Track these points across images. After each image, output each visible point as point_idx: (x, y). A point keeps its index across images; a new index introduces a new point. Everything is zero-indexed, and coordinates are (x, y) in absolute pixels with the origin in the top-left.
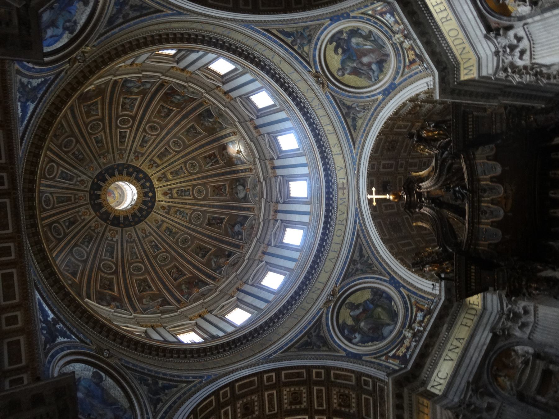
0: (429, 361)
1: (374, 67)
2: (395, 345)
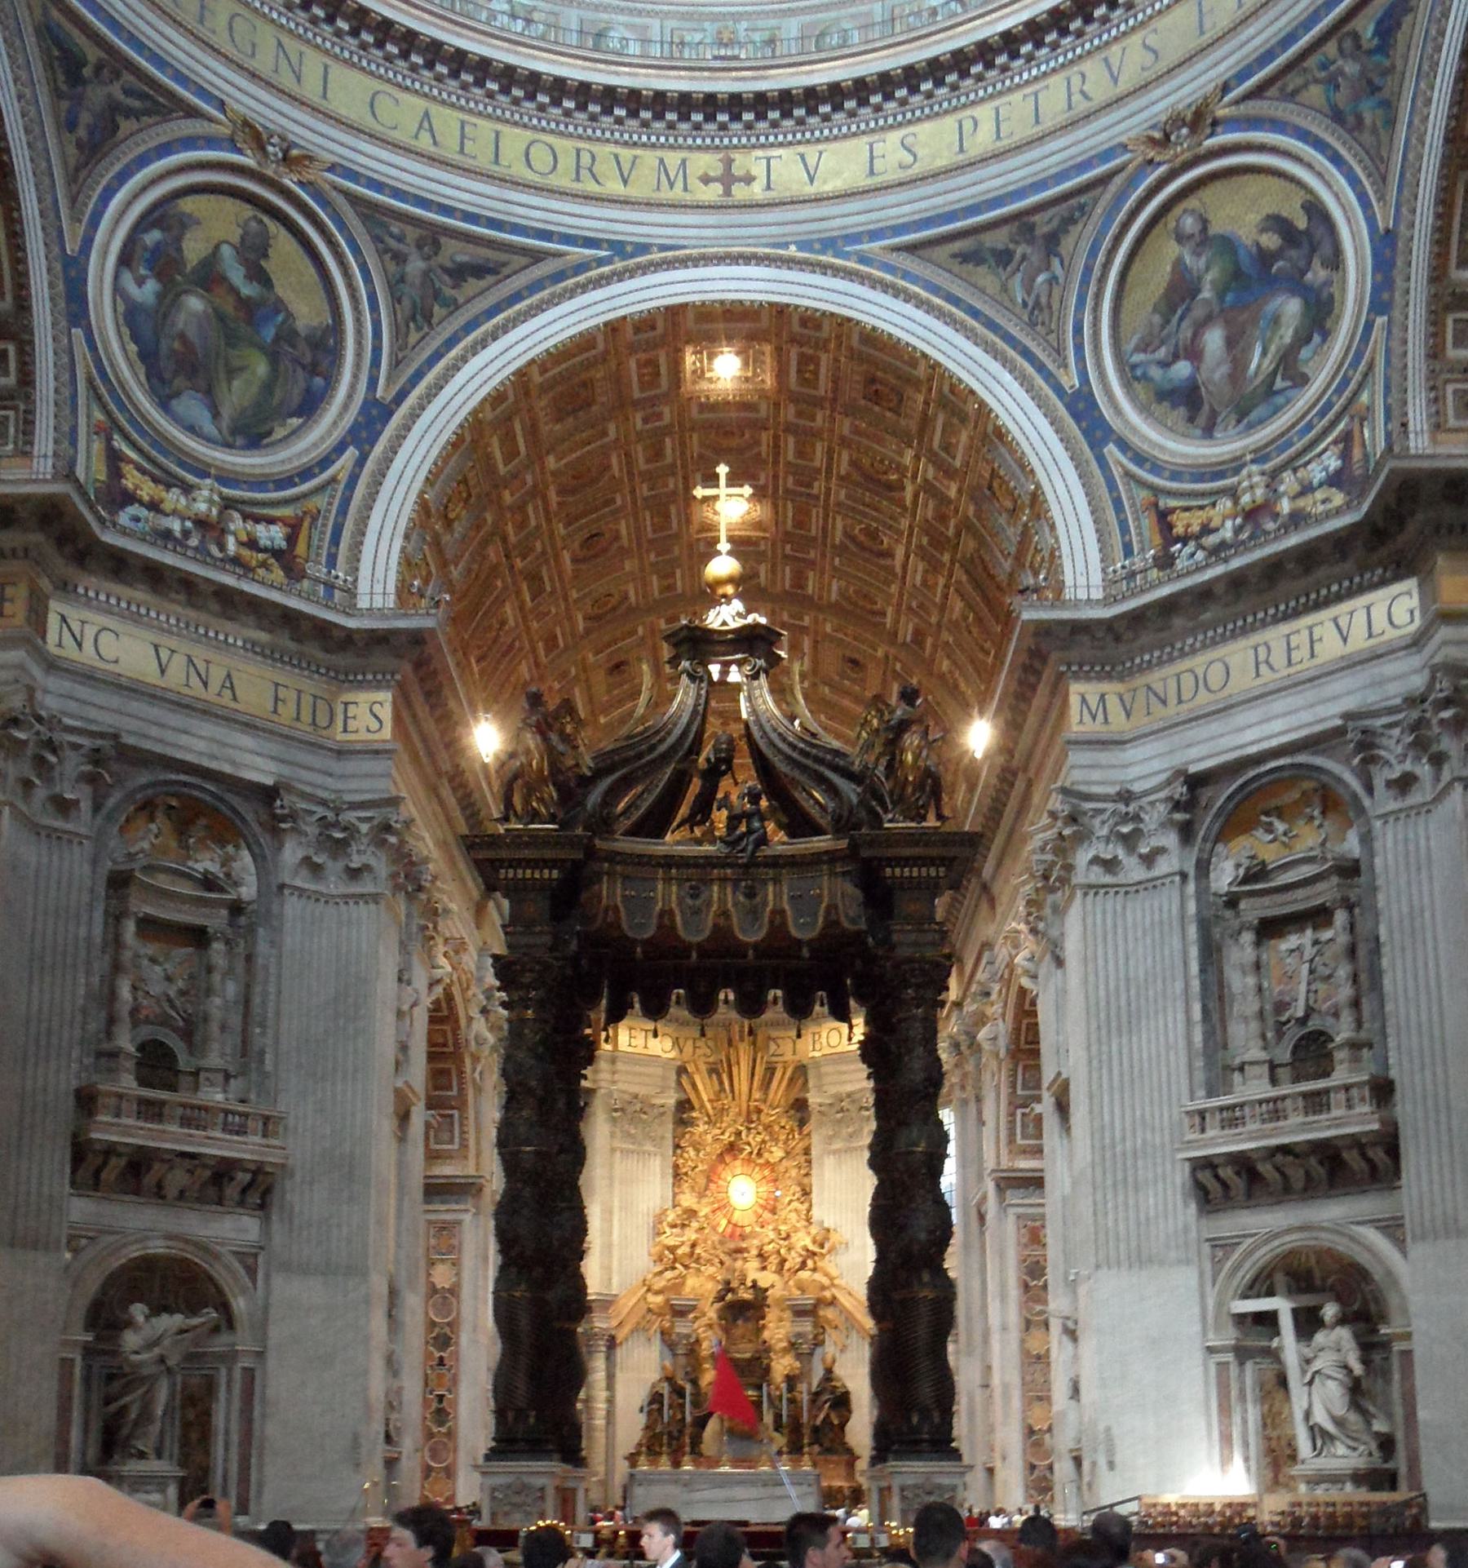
0: (140, 594)
1: (1182, 369)
2: (154, 453)
